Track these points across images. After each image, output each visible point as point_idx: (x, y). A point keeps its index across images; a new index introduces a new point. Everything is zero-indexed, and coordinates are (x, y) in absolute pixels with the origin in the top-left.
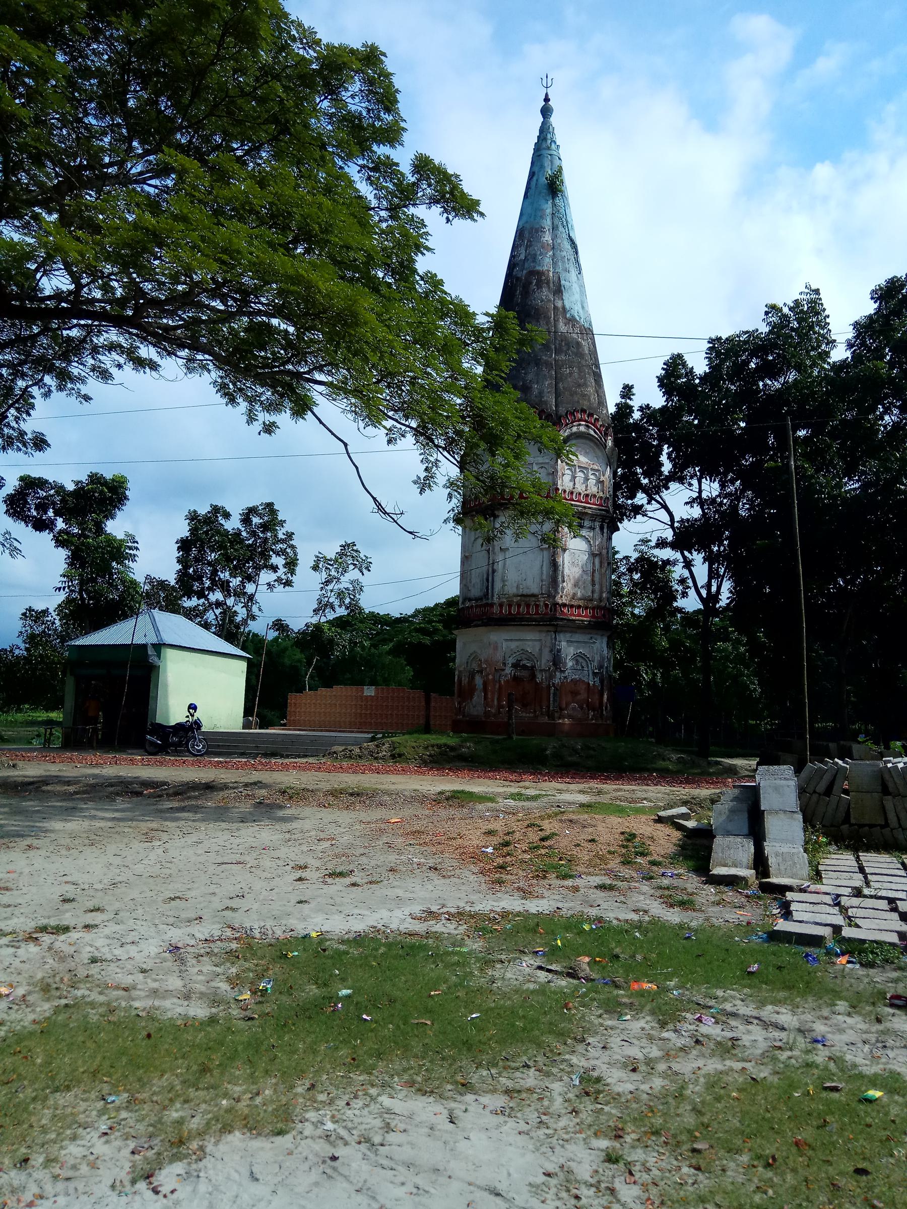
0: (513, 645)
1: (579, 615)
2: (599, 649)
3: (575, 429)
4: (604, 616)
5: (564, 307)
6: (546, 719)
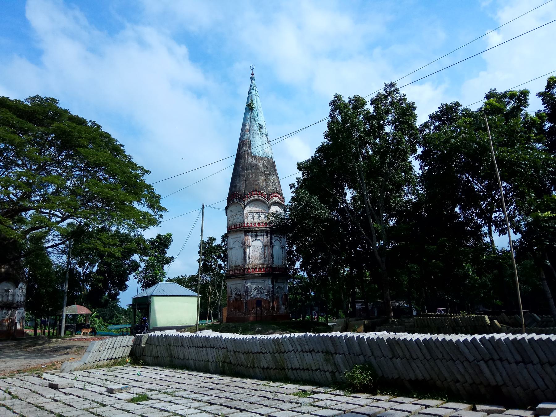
0: (234, 286)
1: (256, 271)
3: (252, 198)
4: (269, 270)
5: (251, 152)
6: (243, 315)
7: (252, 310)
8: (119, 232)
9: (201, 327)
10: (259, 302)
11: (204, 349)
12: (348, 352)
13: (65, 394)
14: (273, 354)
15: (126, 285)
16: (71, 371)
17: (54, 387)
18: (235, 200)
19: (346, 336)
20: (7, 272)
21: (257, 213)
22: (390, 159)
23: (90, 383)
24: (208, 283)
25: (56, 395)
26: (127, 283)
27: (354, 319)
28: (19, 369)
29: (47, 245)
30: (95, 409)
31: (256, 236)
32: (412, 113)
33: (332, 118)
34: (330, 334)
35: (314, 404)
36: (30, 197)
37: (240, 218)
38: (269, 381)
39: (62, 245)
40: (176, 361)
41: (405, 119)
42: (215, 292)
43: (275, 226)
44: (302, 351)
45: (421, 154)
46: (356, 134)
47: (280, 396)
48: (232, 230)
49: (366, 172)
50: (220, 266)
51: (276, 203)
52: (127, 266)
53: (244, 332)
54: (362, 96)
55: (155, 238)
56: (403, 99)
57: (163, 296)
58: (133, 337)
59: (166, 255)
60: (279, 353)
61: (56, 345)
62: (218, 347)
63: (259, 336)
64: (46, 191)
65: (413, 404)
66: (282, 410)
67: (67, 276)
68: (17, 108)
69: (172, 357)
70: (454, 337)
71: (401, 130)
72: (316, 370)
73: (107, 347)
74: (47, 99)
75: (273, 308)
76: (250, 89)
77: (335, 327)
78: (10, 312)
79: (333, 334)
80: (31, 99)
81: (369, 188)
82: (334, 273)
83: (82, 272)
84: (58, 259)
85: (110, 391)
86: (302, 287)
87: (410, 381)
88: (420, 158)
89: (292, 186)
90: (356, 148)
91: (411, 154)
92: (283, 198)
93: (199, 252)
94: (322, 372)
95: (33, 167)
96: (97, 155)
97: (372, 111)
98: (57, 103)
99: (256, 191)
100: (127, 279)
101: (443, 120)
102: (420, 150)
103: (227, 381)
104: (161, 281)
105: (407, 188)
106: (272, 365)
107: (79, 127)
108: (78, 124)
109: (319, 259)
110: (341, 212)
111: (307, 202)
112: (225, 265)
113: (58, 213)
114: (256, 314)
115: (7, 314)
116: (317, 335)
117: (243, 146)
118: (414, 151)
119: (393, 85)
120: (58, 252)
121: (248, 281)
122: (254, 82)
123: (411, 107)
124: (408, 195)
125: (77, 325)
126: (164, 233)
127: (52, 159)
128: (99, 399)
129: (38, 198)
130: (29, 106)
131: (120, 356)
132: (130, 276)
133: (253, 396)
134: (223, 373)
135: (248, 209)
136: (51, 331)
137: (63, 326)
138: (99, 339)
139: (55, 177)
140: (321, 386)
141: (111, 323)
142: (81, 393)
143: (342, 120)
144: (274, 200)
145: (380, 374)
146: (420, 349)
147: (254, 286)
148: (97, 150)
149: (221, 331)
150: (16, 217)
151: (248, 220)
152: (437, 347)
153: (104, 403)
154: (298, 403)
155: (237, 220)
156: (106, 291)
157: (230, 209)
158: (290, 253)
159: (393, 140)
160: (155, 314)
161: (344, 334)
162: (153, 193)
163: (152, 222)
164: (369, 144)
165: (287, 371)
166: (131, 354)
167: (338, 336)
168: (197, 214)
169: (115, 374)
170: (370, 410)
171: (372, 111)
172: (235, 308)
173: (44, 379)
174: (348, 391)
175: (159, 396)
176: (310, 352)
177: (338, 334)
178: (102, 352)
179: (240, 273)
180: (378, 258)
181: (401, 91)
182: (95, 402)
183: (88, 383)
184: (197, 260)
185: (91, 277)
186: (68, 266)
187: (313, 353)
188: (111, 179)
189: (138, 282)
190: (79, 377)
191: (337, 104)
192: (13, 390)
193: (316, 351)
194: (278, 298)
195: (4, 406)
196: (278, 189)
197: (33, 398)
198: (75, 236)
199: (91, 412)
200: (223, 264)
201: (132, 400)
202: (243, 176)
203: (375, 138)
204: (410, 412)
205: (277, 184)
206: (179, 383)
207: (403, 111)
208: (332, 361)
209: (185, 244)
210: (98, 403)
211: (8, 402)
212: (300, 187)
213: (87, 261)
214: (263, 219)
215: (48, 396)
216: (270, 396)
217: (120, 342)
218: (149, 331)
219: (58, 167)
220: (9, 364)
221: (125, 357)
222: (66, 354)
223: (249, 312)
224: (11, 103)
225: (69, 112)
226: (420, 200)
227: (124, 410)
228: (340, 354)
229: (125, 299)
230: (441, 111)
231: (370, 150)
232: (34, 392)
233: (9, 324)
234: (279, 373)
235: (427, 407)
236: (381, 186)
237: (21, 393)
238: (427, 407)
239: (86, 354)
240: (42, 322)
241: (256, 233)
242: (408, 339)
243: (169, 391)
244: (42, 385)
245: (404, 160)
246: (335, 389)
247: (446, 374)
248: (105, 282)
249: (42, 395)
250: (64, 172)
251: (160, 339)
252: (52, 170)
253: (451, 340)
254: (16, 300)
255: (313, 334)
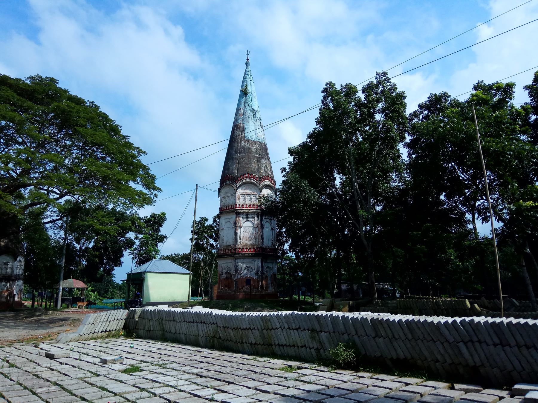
1: (247, 251)
2: (257, 263)
3: (244, 181)
4: (259, 251)
5: (244, 136)
6: (233, 293)
7: (242, 288)
8: (116, 210)
9: (193, 304)
10: (248, 281)
11: (195, 324)
12: (332, 331)
13: (61, 363)
14: (261, 330)
15: (120, 262)
16: (67, 342)
17: (50, 356)
18: (228, 182)
19: (332, 315)
20: (6, 246)
21: (248, 195)
22: (379, 146)
23: (85, 354)
24: (201, 261)
25: (52, 365)
26: (122, 259)
27: (339, 299)
28: (17, 338)
29: (45, 221)
30: (89, 379)
31: (248, 217)
32: (402, 102)
33: (324, 105)
34: (316, 313)
35: (299, 379)
36: (29, 174)
37: (232, 199)
38: (257, 356)
39: (60, 221)
40: (168, 335)
41: (395, 108)
42: (207, 270)
43: (265, 208)
44: (289, 328)
45: (409, 142)
46: (347, 121)
47: (266, 371)
48: (224, 211)
49: (355, 159)
50: (212, 245)
51: (267, 186)
52: (122, 243)
53: (233, 309)
54: (354, 84)
55: (149, 217)
56: (394, 88)
57: (156, 272)
58: (126, 311)
59: (160, 234)
60: (267, 330)
61: (52, 317)
62: (208, 322)
63: (247, 313)
64: (45, 168)
65: (394, 381)
66: (268, 384)
67: (64, 251)
68: (18, 86)
69: (164, 331)
70: (435, 319)
71: (391, 118)
72: (302, 347)
73: (102, 320)
74: (47, 78)
75: (262, 287)
76: (245, 74)
77: (321, 306)
78: (8, 284)
79: (319, 313)
80: (31, 78)
81: (357, 174)
82: (321, 255)
83: (78, 248)
84: (55, 234)
85: (104, 362)
86: (291, 268)
87: (392, 359)
88: (408, 146)
89: (283, 170)
90: (347, 135)
91: (399, 142)
92: (275, 182)
93: (192, 232)
94: (308, 349)
95: (33, 145)
96: (95, 135)
97: (363, 99)
98: (57, 83)
99: (248, 174)
100: (122, 256)
101: (432, 110)
102: (408, 139)
103: (216, 355)
104: (155, 258)
105: (394, 174)
106: (260, 341)
107: (78, 107)
108: (77, 104)
109: (308, 241)
110: (331, 196)
111: (297, 185)
112: (217, 245)
113: (56, 190)
114: (245, 292)
115: (5, 286)
116: (304, 313)
117: (237, 130)
118: (403, 139)
119: (385, 74)
120: (55, 228)
121: (239, 260)
122: (248, 67)
123: (401, 96)
124: (395, 182)
125: (73, 298)
126: (158, 212)
127: (51, 138)
128: (94, 369)
129: (37, 175)
130: (29, 85)
131: (114, 329)
132: (124, 253)
133: (241, 369)
134: (213, 347)
135: (240, 191)
136: (48, 303)
137: (60, 299)
138: (94, 312)
139: (54, 155)
140: (306, 362)
141: (105, 297)
142: (75, 363)
143: (333, 107)
144: (266, 183)
145: (363, 352)
146: (402, 329)
147: (244, 266)
148: (95, 130)
149: (211, 308)
150: (16, 194)
151: (240, 202)
152: (419, 328)
153: (98, 373)
154: (284, 378)
155: (229, 201)
156: (102, 266)
157: (222, 191)
158: (280, 234)
159: (382, 128)
160: (148, 290)
161: (329, 313)
162: (148, 173)
163: (147, 201)
164: (359, 131)
165: (274, 347)
166: (125, 327)
167: (324, 315)
168: (191, 194)
169: (109, 346)
170: (353, 386)
171: (363, 99)
172: (226, 286)
173: (41, 349)
174: (332, 367)
175: (151, 368)
176: (297, 329)
177: (324, 313)
178: (97, 324)
179: (231, 252)
180: (365, 242)
181: (392, 81)
182: (90, 372)
183: (83, 353)
184: (190, 240)
185: (87, 253)
186: (65, 241)
187: (299, 330)
188: (108, 159)
189: (133, 259)
190: (74, 347)
191: (329, 91)
192: (11, 358)
193: (302, 328)
194: (266, 277)
195: (2, 374)
196: (270, 173)
197: (30, 367)
198: (73, 212)
199: (85, 382)
200: (214, 244)
201: (125, 371)
202: (236, 159)
203: (365, 125)
204: (391, 389)
205: (269, 168)
206: (170, 356)
207: (393, 100)
208: (317, 338)
209: (178, 223)
210: (92, 372)
211: (6, 370)
212: (292, 171)
213: (84, 237)
214: (254, 201)
215: (44, 365)
216: (258, 370)
217: (114, 316)
218: (142, 305)
219: (57, 146)
220: (7, 334)
221: (119, 330)
222: (62, 326)
223: (238, 290)
224: (12, 82)
225: (68, 92)
226: (407, 186)
227: (117, 380)
228: (325, 332)
229: (120, 275)
230: (430, 101)
231: (359, 137)
232: (31, 361)
233: (7, 296)
234: (267, 349)
235: (407, 384)
236: (369, 173)
237: (19, 362)
238: (407, 384)
239: (81, 327)
240: (40, 294)
241: (247, 215)
242: (391, 320)
243: (161, 363)
244: (39, 354)
245: (393, 147)
246: (319, 365)
247: (426, 354)
248: (101, 257)
249: (39, 364)
250: (62, 150)
251: (152, 313)
252: (51, 148)
253: (432, 321)
254: (15, 273)
255: (300, 313)
